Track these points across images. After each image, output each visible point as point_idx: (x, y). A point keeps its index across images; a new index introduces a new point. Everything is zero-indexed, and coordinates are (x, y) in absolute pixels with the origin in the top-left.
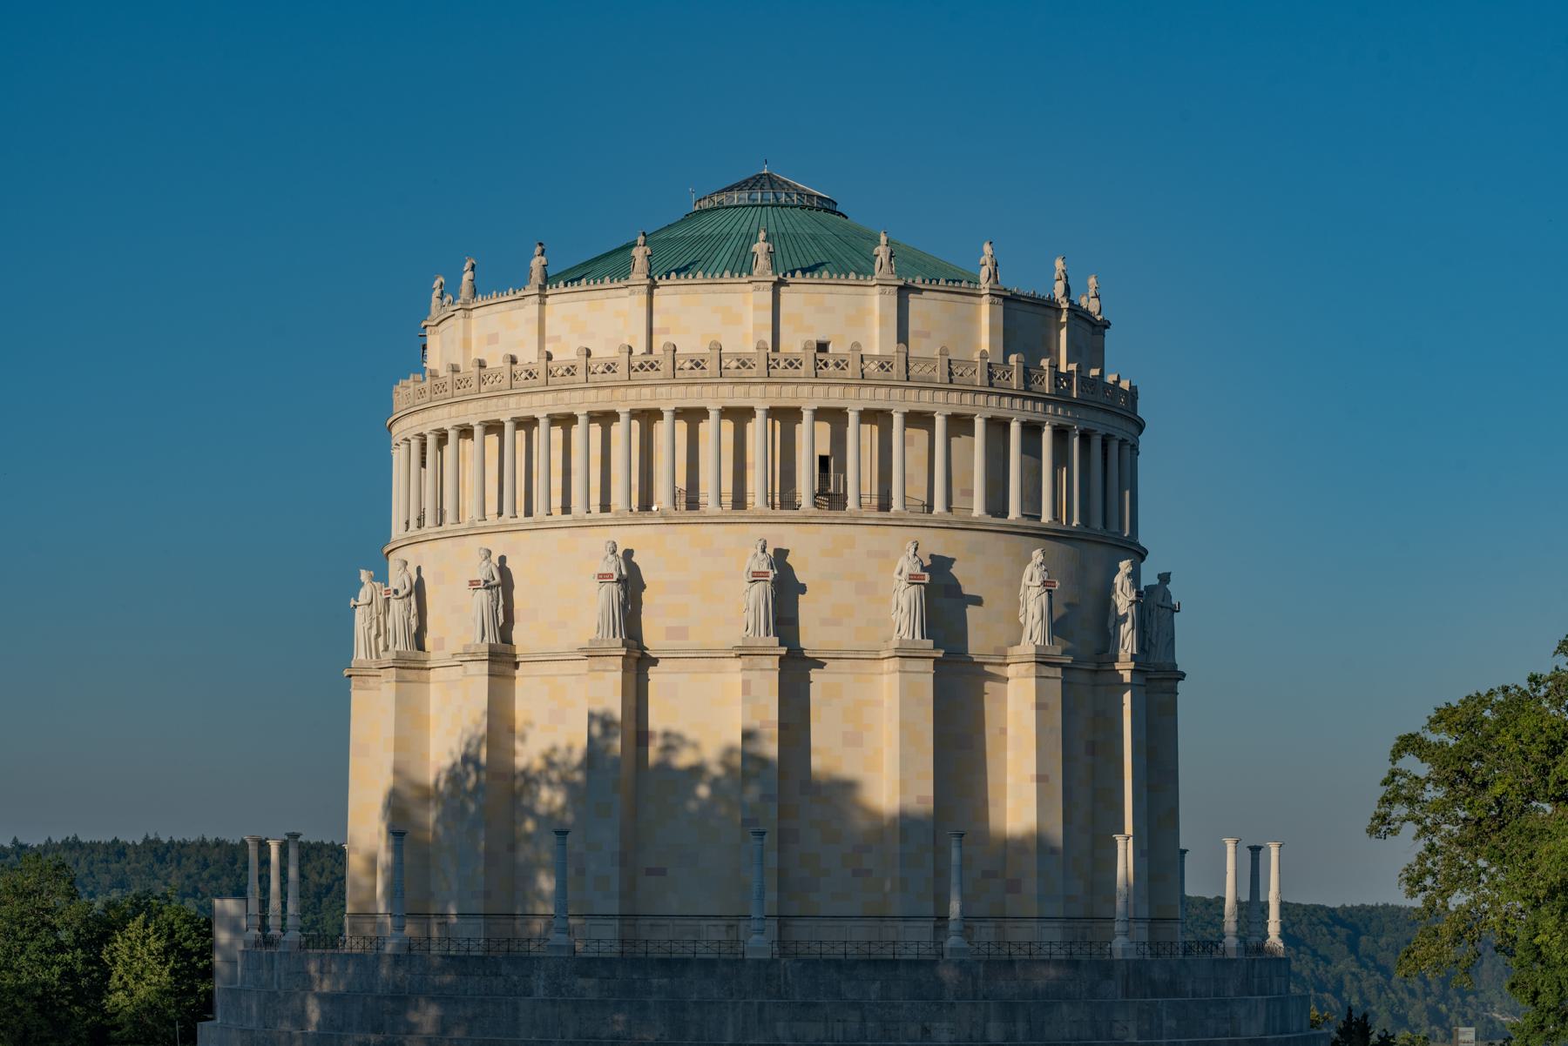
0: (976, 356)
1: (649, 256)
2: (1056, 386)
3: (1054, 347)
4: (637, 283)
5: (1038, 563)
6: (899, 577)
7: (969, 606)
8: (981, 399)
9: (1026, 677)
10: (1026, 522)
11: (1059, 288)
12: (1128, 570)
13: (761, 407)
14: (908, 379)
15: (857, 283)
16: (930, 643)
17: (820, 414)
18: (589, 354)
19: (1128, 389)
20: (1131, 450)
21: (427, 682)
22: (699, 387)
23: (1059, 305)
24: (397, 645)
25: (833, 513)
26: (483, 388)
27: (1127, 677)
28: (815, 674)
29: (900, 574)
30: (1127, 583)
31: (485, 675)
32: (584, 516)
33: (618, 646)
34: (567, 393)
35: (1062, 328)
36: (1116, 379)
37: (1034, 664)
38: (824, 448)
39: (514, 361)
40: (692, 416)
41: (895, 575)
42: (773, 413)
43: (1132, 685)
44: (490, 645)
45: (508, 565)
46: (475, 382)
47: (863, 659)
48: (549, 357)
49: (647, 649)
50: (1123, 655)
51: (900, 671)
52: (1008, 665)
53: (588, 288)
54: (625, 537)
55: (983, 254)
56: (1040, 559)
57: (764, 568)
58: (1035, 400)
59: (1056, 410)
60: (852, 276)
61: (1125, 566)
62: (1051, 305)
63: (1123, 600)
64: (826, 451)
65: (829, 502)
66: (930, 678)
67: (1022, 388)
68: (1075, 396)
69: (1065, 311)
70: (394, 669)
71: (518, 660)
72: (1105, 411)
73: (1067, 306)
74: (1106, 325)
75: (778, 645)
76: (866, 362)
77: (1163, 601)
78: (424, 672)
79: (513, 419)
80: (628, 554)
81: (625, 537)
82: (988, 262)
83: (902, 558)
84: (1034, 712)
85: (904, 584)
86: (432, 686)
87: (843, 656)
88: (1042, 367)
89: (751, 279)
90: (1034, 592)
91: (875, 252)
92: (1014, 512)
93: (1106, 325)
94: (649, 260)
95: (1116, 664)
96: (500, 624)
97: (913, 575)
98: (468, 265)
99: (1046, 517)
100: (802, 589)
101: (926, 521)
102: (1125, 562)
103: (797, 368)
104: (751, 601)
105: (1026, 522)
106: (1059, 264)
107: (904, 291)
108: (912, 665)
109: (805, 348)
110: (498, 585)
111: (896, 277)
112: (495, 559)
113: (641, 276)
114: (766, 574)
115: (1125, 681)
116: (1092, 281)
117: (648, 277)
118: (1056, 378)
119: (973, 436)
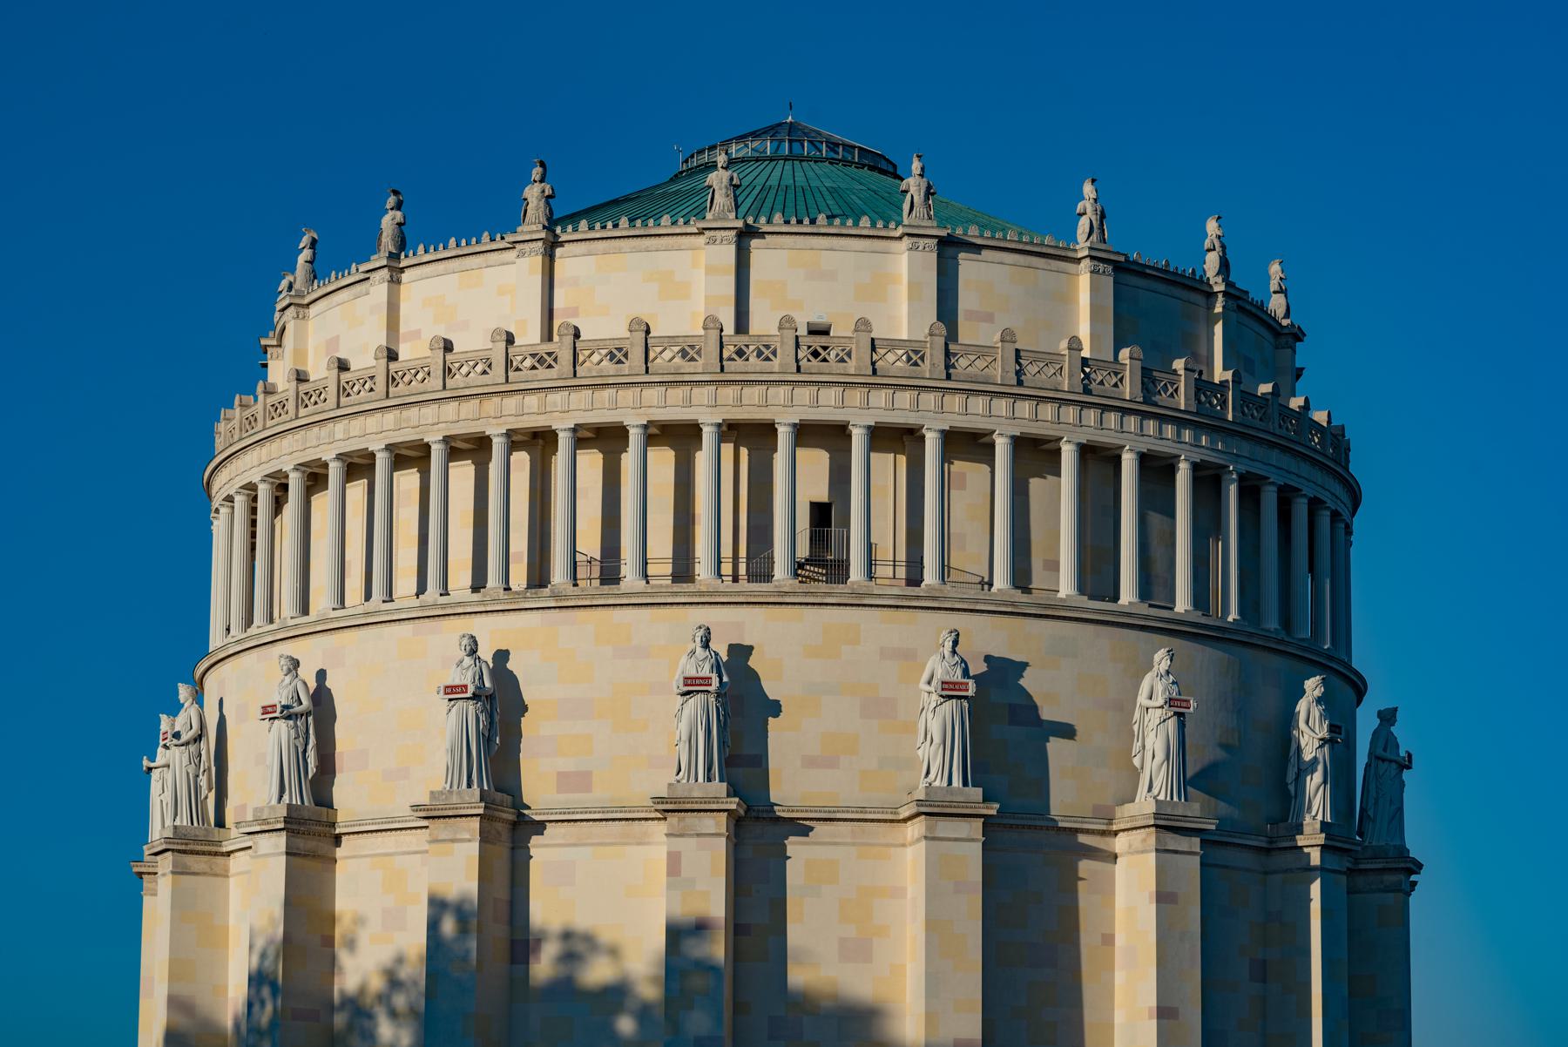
0: (1063, 346)
1: (549, 197)
2: (1199, 402)
3: (1203, 351)
4: (528, 238)
5: (1163, 671)
6: (928, 688)
7: (1051, 738)
8: (1070, 413)
9: (1142, 852)
10: (1144, 609)
11: (1212, 261)
12: (1317, 693)
13: (709, 420)
14: (949, 377)
16: (976, 793)
17: (807, 433)
18: (448, 347)
19: (1325, 424)
20: (1332, 522)
21: (225, 875)
23: (1211, 286)
24: (178, 817)
25: (823, 587)
26: (302, 412)
27: (1315, 857)
28: (794, 846)
29: (929, 683)
30: (1316, 712)
31: (279, 854)
32: (436, 600)
33: (473, 801)
34: (414, 410)
36: (1302, 404)
37: (1153, 829)
38: (815, 487)
39: (343, 366)
40: (608, 438)
41: (923, 686)
42: (733, 431)
43: (1322, 870)
44: (290, 806)
45: (328, 684)
46: (291, 406)
47: (872, 821)
48: (392, 356)
49: (529, 808)
50: (1309, 824)
51: (926, 838)
52: (1116, 833)
54: (492, 633)
55: (1083, 199)
57: (706, 671)
58: (1162, 419)
59: (1197, 438)
60: (865, 221)
61: (1313, 686)
62: (1197, 287)
63: (1310, 736)
64: (822, 495)
65: (826, 574)
66: (977, 848)
67: (1141, 400)
68: (1230, 418)
69: (1220, 296)
70: (170, 853)
71: (337, 832)
72: (1284, 449)
73: (1222, 288)
74: (1297, 335)
75: (724, 794)
76: (882, 351)
77: (1385, 750)
78: (220, 860)
79: (340, 457)
80: (502, 656)
81: (492, 633)
82: (1089, 210)
83: (933, 657)
84: (1152, 908)
85: (934, 697)
86: (232, 881)
87: (839, 816)
88: (1175, 372)
89: (702, 225)
92: (1128, 593)
93: (1297, 335)
94: (547, 203)
95: (1298, 837)
96: (310, 776)
97: (946, 683)
98: (305, 240)
99: (1182, 604)
100: (775, 708)
101: (977, 601)
102: (1312, 680)
103: (768, 359)
104: (684, 727)
105: (1144, 609)
106: (1212, 227)
107: (949, 248)
108: (947, 828)
109: (780, 328)
110: (308, 714)
111: (935, 224)
112: (308, 674)
113: (534, 227)
115: (1312, 864)
116: (1275, 269)
117: (544, 227)
118: (1198, 390)
119: (1060, 476)
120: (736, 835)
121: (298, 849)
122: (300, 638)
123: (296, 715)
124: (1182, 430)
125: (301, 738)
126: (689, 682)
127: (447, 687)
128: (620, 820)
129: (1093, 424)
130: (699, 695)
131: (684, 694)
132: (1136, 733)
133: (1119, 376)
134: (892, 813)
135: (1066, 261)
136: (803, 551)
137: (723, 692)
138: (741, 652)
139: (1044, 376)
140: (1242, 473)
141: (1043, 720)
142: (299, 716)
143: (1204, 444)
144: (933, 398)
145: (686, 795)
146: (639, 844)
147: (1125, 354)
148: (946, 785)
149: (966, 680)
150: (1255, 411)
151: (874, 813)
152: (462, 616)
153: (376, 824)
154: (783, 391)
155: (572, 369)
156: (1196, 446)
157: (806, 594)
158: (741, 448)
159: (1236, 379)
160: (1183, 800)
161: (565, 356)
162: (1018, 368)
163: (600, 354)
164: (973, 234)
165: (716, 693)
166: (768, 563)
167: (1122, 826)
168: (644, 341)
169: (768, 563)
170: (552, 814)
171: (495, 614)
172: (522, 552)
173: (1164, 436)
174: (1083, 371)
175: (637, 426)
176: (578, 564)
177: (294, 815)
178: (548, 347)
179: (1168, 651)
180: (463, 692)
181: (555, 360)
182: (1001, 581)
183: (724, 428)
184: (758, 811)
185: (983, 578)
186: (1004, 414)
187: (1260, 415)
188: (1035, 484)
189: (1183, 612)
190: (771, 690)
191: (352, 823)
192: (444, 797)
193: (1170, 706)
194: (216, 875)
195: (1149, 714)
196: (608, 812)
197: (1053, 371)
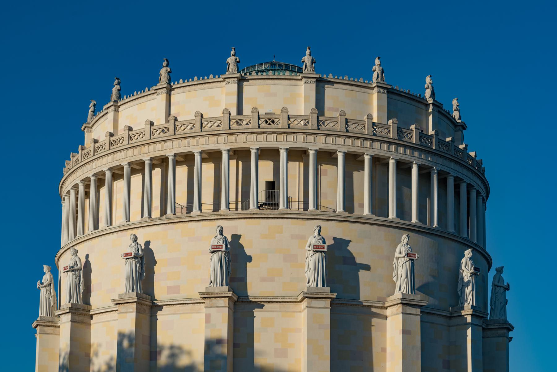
3: (424, 127)
7: (360, 270)
8: (368, 144)
9: (397, 314)
11: (428, 93)
14: (319, 129)
15: (290, 77)
16: (328, 289)
22: (188, 140)
28: (258, 313)
29: (309, 247)
34: (119, 153)
35: (430, 116)
41: (307, 248)
44: (72, 304)
45: (89, 259)
47: (288, 302)
49: (157, 300)
51: (307, 307)
53: (138, 96)
56: (406, 241)
58: (406, 147)
59: (420, 155)
61: (468, 253)
62: (422, 101)
64: (271, 179)
66: (328, 312)
68: (434, 148)
69: (431, 105)
71: (91, 314)
72: (456, 163)
73: (432, 102)
78: (57, 329)
80: (148, 243)
85: (311, 252)
87: (274, 300)
88: (411, 129)
90: (402, 260)
91: (303, 60)
92: (392, 214)
96: (81, 293)
97: (316, 246)
99: (414, 219)
100: (250, 259)
106: (428, 80)
107: (321, 83)
108: (315, 303)
110: (81, 269)
114: (220, 247)
120: (234, 308)
121: (75, 320)
122: (81, 243)
123: (76, 270)
124: (414, 152)
125: (77, 279)
126: (214, 247)
127: (125, 254)
128: (190, 303)
129: (377, 148)
130: (218, 253)
131: (213, 252)
132: (394, 268)
133: (388, 130)
134: (295, 299)
135: (368, 89)
136: (262, 198)
137: (227, 251)
138: (236, 237)
139: (357, 129)
140: (439, 170)
141: (357, 263)
142: (77, 270)
143: (423, 158)
144: (312, 137)
145: (212, 291)
146: (197, 313)
147: (390, 122)
148: (315, 286)
149: (324, 245)
150: (444, 148)
151: (288, 299)
152: (134, 229)
153: (103, 309)
154: (253, 136)
155: (174, 132)
156: (420, 158)
157: (261, 213)
158: (239, 161)
159: (436, 134)
160: (413, 294)
161: (172, 128)
162: (347, 126)
163: (184, 126)
164: (330, 77)
165: (224, 251)
166: (248, 203)
167: (389, 305)
168: (200, 120)
169: (248, 203)
170: (165, 302)
171: (145, 227)
172: (158, 206)
173: (407, 154)
174: (373, 128)
175: (198, 153)
176: (176, 207)
177: (74, 307)
178: (167, 125)
179: (407, 235)
180: (130, 255)
181: (168, 130)
182: (340, 209)
183: (231, 153)
184: (243, 298)
185: (334, 210)
186: (341, 144)
187: (447, 149)
188: (356, 174)
189: (415, 222)
190: (248, 252)
191: (95, 310)
192: (123, 296)
193: (408, 256)
194: (56, 334)
195: (399, 260)
196: (185, 300)
197: (361, 127)
